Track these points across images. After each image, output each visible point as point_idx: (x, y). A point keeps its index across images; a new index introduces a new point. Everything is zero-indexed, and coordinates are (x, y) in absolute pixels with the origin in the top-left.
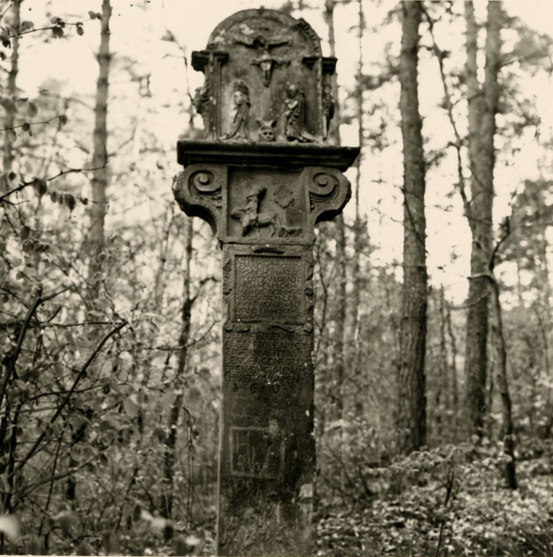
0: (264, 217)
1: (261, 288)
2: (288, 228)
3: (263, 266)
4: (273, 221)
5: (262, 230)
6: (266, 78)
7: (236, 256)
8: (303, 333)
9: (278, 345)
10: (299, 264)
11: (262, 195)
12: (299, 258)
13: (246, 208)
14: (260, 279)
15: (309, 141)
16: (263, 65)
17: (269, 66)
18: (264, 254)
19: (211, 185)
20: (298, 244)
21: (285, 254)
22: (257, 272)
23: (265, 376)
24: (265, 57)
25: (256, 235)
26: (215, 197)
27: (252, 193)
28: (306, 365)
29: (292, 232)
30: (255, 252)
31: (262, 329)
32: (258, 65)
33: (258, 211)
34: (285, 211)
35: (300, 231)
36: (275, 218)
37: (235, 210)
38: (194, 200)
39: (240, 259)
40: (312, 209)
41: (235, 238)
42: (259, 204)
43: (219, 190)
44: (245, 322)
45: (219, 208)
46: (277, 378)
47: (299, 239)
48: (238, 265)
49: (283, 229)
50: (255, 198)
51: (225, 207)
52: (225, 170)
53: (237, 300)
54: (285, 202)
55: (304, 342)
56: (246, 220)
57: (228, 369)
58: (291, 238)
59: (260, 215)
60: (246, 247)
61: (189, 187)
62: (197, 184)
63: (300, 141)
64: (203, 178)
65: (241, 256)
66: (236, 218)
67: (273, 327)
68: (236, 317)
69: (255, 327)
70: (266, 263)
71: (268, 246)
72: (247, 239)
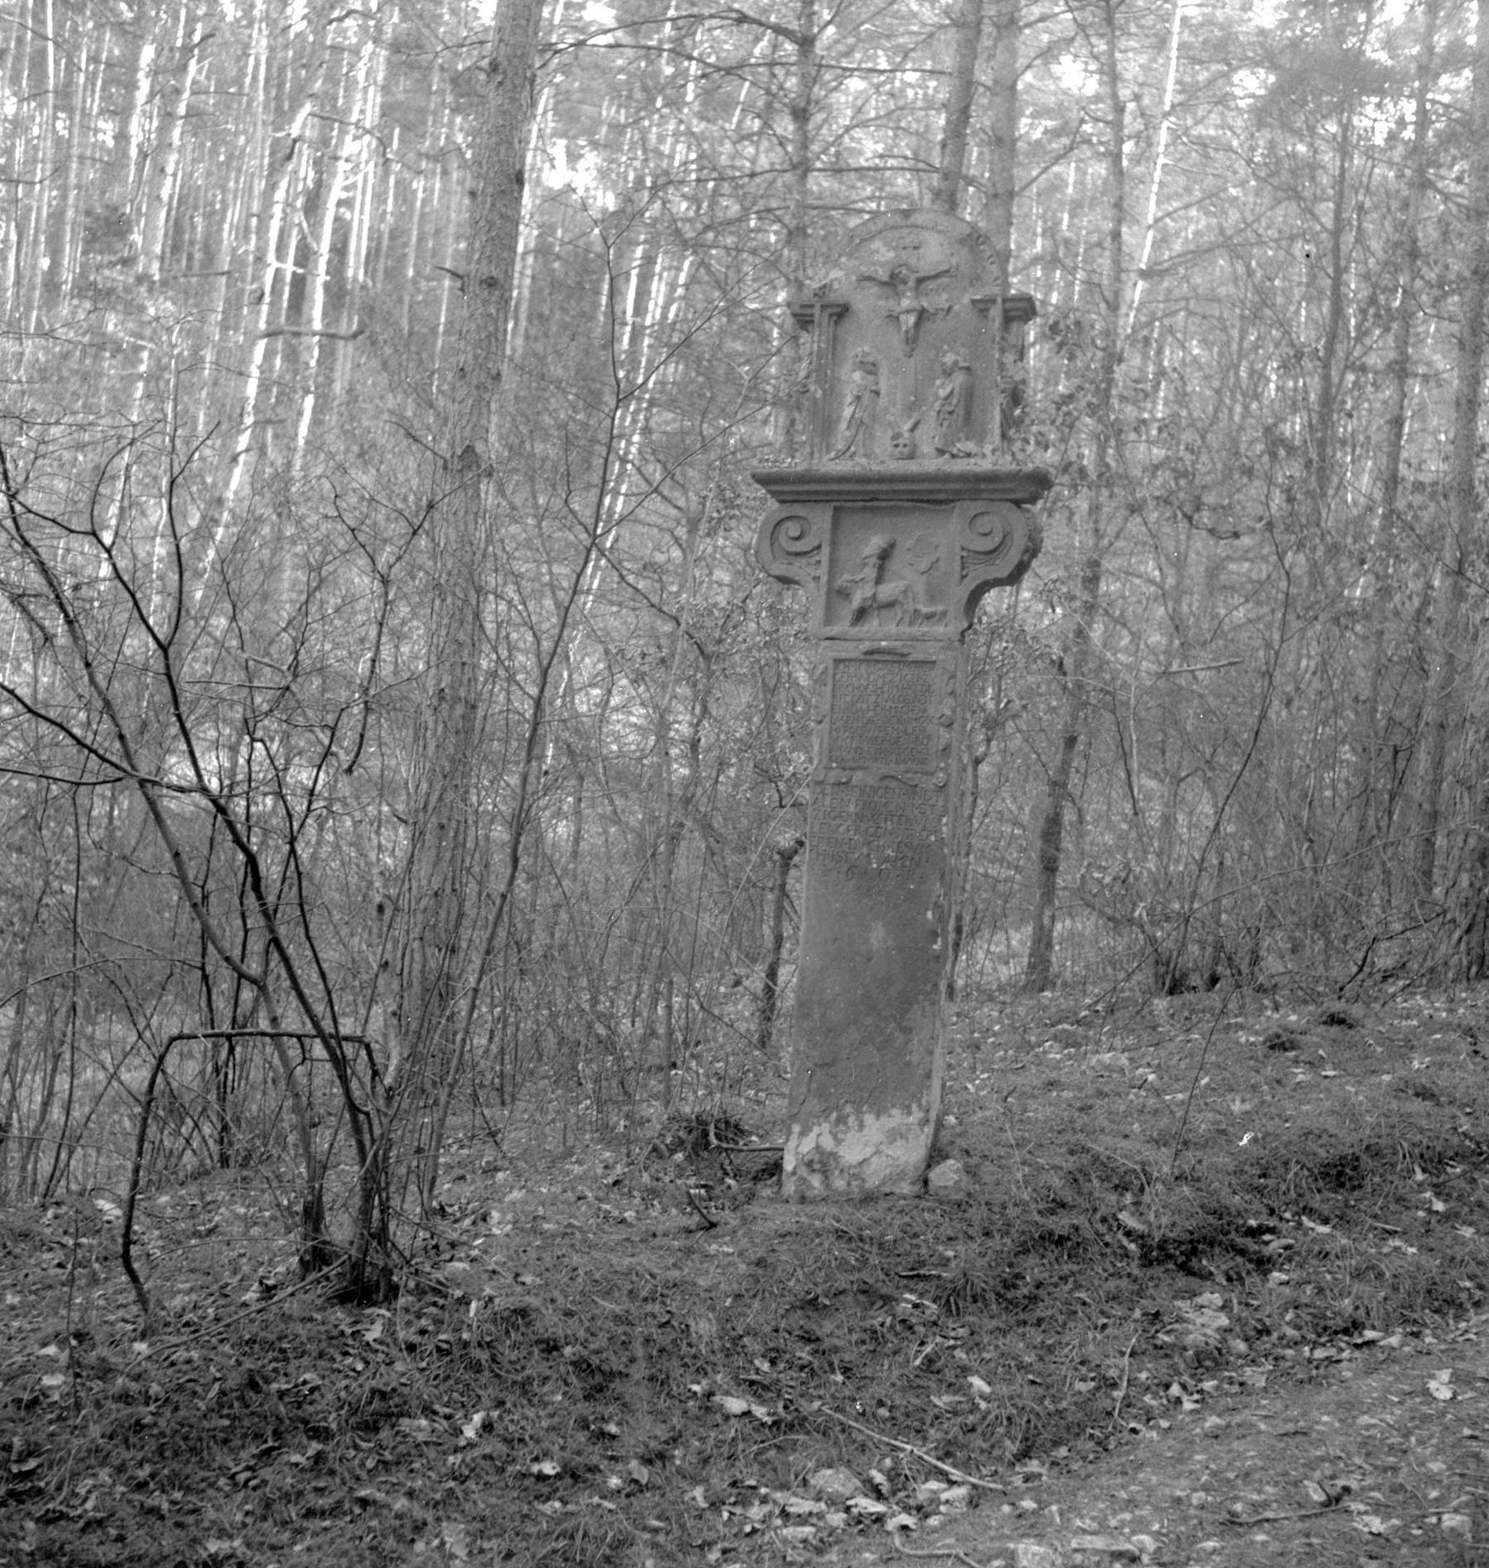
0: (887, 591)
5: (884, 612)
6: (907, 341)
7: (838, 661)
9: (892, 807)
11: (885, 556)
14: (872, 699)
15: (968, 455)
16: (903, 318)
24: (906, 303)
25: (872, 625)
27: (868, 551)
31: (871, 781)
32: (893, 318)
33: (879, 580)
35: (944, 613)
36: (905, 592)
37: (843, 580)
38: (779, 568)
40: (963, 577)
41: (834, 630)
42: (881, 569)
43: (819, 547)
45: (816, 578)
46: (887, 859)
47: (940, 629)
50: (874, 560)
51: (824, 579)
62: (782, 539)
63: (954, 456)
64: (793, 529)
66: (844, 594)
67: (884, 778)
68: (830, 759)
69: (858, 776)
72: (855, 631)
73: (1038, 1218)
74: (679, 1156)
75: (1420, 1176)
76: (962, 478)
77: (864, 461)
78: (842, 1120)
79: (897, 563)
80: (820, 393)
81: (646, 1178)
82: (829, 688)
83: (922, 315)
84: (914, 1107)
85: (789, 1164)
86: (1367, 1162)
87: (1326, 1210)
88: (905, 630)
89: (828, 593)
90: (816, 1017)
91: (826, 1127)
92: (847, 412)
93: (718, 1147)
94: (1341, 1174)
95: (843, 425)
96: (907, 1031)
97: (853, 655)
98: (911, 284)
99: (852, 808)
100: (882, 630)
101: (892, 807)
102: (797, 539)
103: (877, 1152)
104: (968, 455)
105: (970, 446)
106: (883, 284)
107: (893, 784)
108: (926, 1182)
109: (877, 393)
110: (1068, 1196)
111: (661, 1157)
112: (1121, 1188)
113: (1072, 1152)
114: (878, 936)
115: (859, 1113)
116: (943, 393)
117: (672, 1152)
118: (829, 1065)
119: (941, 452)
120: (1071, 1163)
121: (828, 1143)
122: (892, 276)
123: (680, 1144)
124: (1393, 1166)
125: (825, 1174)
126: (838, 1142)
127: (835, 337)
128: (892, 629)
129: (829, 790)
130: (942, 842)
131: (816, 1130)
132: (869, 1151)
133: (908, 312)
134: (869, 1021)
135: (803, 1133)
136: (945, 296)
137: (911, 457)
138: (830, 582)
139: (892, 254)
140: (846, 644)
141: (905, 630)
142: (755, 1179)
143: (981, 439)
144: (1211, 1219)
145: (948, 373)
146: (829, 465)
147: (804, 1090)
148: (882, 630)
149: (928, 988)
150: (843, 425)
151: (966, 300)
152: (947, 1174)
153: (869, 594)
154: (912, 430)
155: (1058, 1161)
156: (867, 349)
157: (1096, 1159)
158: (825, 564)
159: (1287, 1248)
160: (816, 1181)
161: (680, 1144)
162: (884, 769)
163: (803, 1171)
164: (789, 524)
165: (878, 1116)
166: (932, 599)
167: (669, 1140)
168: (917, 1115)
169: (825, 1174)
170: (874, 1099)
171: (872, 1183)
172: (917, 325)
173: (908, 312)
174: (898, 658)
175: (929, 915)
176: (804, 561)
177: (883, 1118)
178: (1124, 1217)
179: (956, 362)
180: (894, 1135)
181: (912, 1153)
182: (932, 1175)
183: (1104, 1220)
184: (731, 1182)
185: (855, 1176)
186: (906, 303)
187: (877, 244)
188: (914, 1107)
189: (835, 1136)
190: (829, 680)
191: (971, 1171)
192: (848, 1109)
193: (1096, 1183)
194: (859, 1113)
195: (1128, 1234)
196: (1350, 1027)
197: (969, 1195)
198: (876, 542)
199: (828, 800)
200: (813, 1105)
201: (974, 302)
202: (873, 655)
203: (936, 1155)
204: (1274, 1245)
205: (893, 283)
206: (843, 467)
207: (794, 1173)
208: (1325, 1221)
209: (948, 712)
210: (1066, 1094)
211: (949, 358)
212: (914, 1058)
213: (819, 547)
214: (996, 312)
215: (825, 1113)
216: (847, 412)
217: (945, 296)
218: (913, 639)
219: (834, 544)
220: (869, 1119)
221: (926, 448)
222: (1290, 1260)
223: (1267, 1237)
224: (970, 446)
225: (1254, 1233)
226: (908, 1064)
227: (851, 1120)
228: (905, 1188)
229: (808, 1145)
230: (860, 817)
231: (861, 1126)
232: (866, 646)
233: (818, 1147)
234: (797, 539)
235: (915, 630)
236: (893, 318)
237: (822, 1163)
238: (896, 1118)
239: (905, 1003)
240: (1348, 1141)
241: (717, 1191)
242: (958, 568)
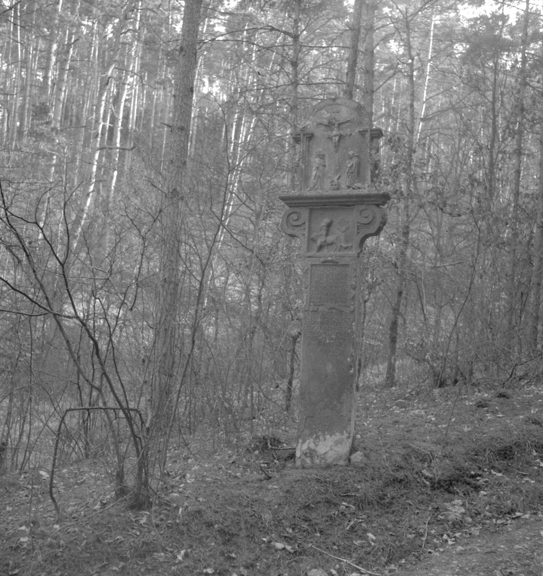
0: (330, 239)
6: (335, 147)
7: (312, 265)
11: (329, 225)
15: (359, 188)
16: (334, 138)
17: (337, 138)
18: (327, 263)
24: (335, 133)
25: (325, 251)
29: (346, 248)
33: (327, 235)
34: (344, 234)
35: (352, 247)
36: (337, 239)
37: (313, 235)
38: (290, 231)
43: (304, 223)
45: (304, 235)
46: (333, 339)
47: (350, 253)
49: (341, 246)
50: (325, 228)
51: (306, 235)
52: (308, 211)
54: (344, 229)
56: (319, 242)
58: (344, 253)
60: (317, 259)
62: (291, 221)
63: (354, 189)
64: (295, 217)
66: (314, 240)
68: (310, 302)
69: (321, 308)
73: (392, 473)
74: (257, 452)
75: (535, 454)
76: (357, 196)
77: (320, 191)
78: (317, 437)
79: (332, 229)
80: (303, 166)
81: (244, 460)
82: (309, 275)
83: (341, 137)
84: (345, 432)
85: (298, 454)
87: (500, 467)
88: (338, 253)
89: (308, 240)
90: (307, 398)
91: (312, 440)
92: (314, 173)
93: (271, 448)
94: (505, 454)
95: (313, 178)
97: (318, 263)
98: (336, 125)
99: (319, 320)
100: (329, 254)
102: (297, 220)
103: (331, 449)
104: (359, 188)
105: (359, 185)
106: (326, 126)
107: (334, 311)
108: (349, 460)
109: (325, 166)
110: (403, 464)
111: (250, 452)
112: (423, 461)
113: (404, 448)
114: (330, 368)
116: (349, 165)
117: (254, 450)
119: (349, 187)
120: (404, 452)
121: (312, 446)
122: (329, 123)
123: (257, 448)
124: (525, 450)
125: (312, 457)
126: (316, 445)
127: (309, 146)
128: (332, 253)
129: (310, 313)
130: (353, 333)
131: (308, 441)
132: (328, 449)
133: (335, 136)
134: (327, 399)
135: (303, 442)
136: (349, 130)
137: (338, 189)
138: (309, 236)
139: (329, 115)
140: (315, 259)
141: (338, 253)
142: (286, 460)
143: (363, 181)
144: (457, 472)
145: (351, 158)
146: (307, 193)
147: (303, 426)
148: (329, 254)
149: (349, 387)
150: (313, 178)
151: (357, 131)
152: (357, 457)
153: (323, 240)
154: (338, 179)
155: (399, 451)
156: (320, 150)
157: (413, 450)
159: (486, 482)
160: (308, 461)
161: (257, 448)
162: (331, 305)
163: (303, 457)
165: (331, 436)
166: (347, 242)
167: (253, 446)
168: (346, 435)
169: (312, 457)
170: (329, 428)
171: (329, 461)
172: (339, 141)
173: (335, 136)
174: (335, 263)
175: (349, 359)
176: (299, 228)
177: (333, 437)
178: (424, 471)
179: (353, 154)
180: (337, 443)
181: (344, 449)
182: (352, 457)
183: (417, 473)
184: (276, 461)
185: (323, 458)
186: (335, 133)
187: (323, 111)
188: (345, 432)
190: (309, 272)
191: (366, 456)
192: (320, 433)
193: (413, 459)
194: (324, 435)
195: (426, 478)
196: (508, 398)
197: (366, 465)
198: (326, 221)
199: (310, 317)
200: (307, 432)
201: (359, 131)
202: (325, 263)
203: (353, 450)
204: (481, 481)
205: (330, 125)
206: (313, 193)
207: (300, 458)
208: (500, 471)
210: (402, 426)
211: (351, 153)
213: (304, 223)
214: (368, 135)
215: (311, 435)
216: (314, 173)
217: (349, 130)
218: (341, 256)
219: (310, 221)
220: (328, 437)
221: (343, 186)
222: (487, 486)
223: (478, 478)
224: (359, 185)
225: (473, 477)
226: (342, 416)
227: (321, 438)
228: (342, 463)
229: (305, 447)
230: (322, 323)
231: (325, 439)
232: (322, 260)
233: (309, 448)
234: (297, 220)
236: (330, 138)
237: (311, 454)
238: (338, 436)
240: (508, 441)
241: (271, 465)
242: (356, 229)
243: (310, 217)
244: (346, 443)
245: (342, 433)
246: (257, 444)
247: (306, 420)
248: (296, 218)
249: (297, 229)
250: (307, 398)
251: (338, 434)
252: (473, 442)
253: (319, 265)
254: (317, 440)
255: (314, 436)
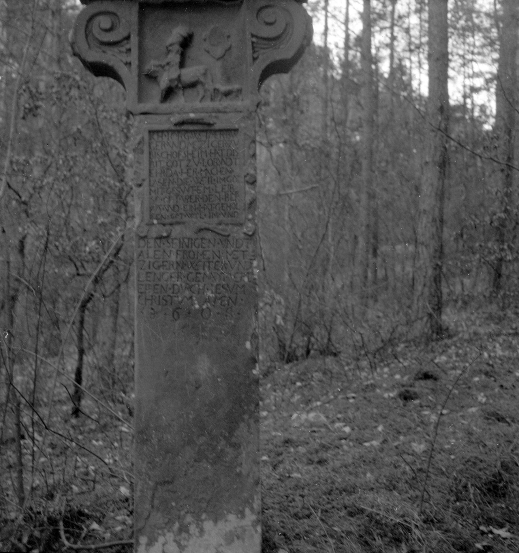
0: (189, 73)
1: (185, 176)
2: (223, 88)
3: (190, 143)
4: (202, 79)
5: (189, 92)
7: (151, 132)
8: (242, 235)
9: (208, 254)
10: (236, 139)
11: (186, 43)
12: (236, 130)
13: (164, 63)
14: (184, 163)
18: (185, 127)
19: (112, 33)
20: (237, 111)
21: (217, 127)
22: (178, 154)
23: (191, 298)
25: (180, 101)
26: (123, 49)
28: (246, 279)
29: (227, 94)
30: (176, 125)
31: (189, 233)
33: (182, 65)
34: (219, 63)
35: (239, 91)
36: (205, 74)
37: (151, 65)
38: (95, 56)
39: (155, 136)
40: (255, 59)
41: (147, 106)
42: (183, 56)
43: (128, 38)
44: (164, 225)
46: (208, 300)
47: (239, 103)
48: (153, 145)
49: (216, 90)
50: (177, 47)
51: (135, 63)
52: (135, 9)
53: (153, 194)
54: (219, 51)
55: (243, 248)
56: (164, 81)
57: (143, 290)
58: (226, 103)
59: (184, 71)
60: (165, 118)
61: (87, 36)
62: (96, 31)
64: (105, 22)
65: (157, 132)
66: (152, 77)
67: (200, 230)
68: (151, 217)
69: (176, 231)
70: (191, 140)
71: (192, 115)
78: (184, 529)
79: (193, 52)
84: (247, 511)
86: (506, 476)
89: (139, 76)
90: (155, 441)
91: (170, 536)
96: (236, 446)
97: (166, 127)
99: (173, 258)
101: (208, 254)
107: (208, 235)
113: (351, 514)
114: (204, 367)
115: (199, 520)
118: (168, 482)
128: (198, 104)
129: (152, 243)
130: (254, 283)
131: (161, 539)
134: (201, 440)
140: (158, 118)
141: (208, 104)
147: (148, 506)
148: (186, 106)
153: (174, 75)
155: (346, 526)
157: (370, 516)
158: (135, 52)
164: (101, 18)
165: (216, 521)
166: (228, 80)
167: (25, 540)
168: (250, 517)
174: (204, 127)
175: (248, 345)
176: (116, 49)
177: (221, 524)
188: (247, 511)
189: (179, 545)
192: (189, 518)
193: (379, 541)
194: (199, 520)
198: (178, 32)
199: (151, 253)
200: (158, 518)
209: (252, 172)
210: (302, 449)
212: (244, 469)
213: (128, 38)
215: (169, 523)
218: (219, 111)
219: (141, 34)
220: (208, 525)
226: (239, 475)
227: (193, 529)
230: (181, 265)
231: (202, 531)
232: (175, 119)
235: (217, 104)
239: (232, 422)
240: (493, 461)
242: (250, 51)
243: (141, 23)
244: (252, 536)
245: (242, 514)
246: (37, 534)
247: (155, 489)
248: (108, 26)
249: (110, 52)
250: (155, 441)
251: (232, 517)
252: (443, 473)
253: (168, 131)
254: (184, 535)
255: (177, 525)
